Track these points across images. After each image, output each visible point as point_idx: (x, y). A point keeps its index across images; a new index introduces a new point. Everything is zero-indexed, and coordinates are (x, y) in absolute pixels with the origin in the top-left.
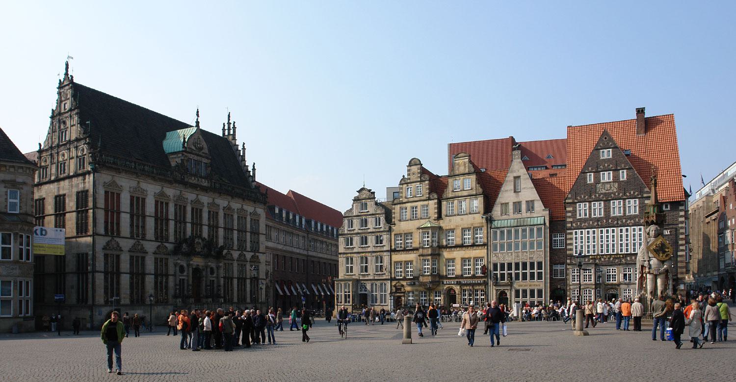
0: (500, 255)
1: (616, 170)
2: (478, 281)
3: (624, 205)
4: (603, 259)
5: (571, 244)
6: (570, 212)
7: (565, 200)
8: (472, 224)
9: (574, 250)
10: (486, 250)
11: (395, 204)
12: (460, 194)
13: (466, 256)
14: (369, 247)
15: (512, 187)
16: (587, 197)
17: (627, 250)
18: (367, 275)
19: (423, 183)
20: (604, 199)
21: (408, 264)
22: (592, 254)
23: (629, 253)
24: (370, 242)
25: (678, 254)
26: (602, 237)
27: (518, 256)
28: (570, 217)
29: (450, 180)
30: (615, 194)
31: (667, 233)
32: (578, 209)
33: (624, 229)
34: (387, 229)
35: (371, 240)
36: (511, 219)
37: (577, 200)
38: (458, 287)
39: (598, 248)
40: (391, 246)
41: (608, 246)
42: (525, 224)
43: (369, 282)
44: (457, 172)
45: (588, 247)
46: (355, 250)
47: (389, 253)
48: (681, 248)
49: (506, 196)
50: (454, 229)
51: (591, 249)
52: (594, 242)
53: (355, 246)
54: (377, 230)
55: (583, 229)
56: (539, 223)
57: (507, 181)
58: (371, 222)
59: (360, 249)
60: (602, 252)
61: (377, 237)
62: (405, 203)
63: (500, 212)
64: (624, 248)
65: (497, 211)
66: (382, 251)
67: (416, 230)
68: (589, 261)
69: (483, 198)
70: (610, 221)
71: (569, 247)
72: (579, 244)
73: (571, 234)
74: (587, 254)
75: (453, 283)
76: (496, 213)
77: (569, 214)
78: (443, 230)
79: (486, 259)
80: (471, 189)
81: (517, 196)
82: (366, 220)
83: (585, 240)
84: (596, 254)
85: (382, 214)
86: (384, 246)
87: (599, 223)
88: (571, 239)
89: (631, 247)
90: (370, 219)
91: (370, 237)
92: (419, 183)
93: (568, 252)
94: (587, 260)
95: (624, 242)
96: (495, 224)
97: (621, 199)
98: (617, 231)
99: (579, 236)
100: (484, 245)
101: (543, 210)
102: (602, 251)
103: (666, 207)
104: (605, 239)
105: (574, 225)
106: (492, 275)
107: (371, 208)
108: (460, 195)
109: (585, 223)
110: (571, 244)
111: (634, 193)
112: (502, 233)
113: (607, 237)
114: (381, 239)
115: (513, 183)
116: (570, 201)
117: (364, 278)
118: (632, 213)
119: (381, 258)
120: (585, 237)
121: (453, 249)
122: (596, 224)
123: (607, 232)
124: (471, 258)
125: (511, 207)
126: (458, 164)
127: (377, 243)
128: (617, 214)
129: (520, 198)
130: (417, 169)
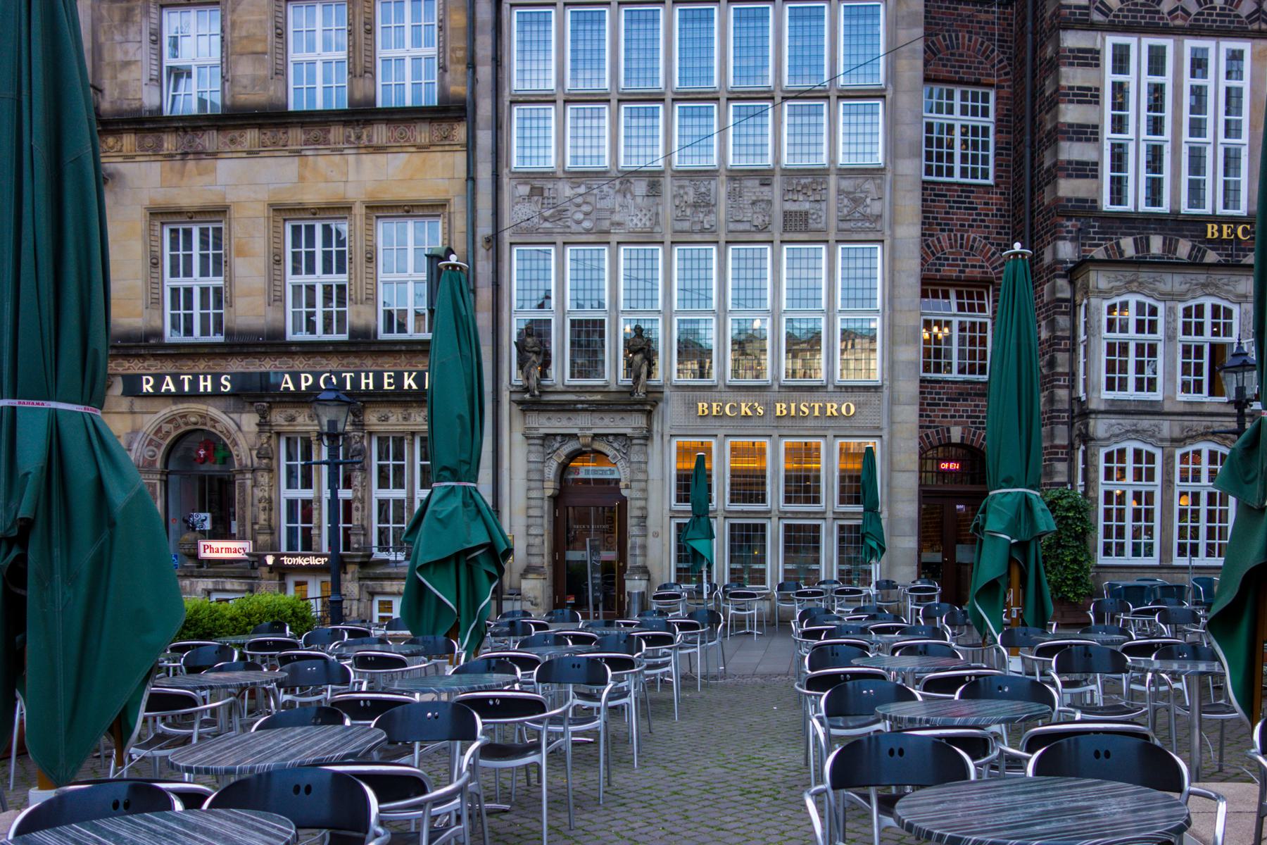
0: (566, 190)
2: (399, 378)
5: (1088, 133)
9: (1106, 173)
10: (460, 158)
13: (313, 195)
27: (704, 203)
38: (249, 421)
71: (1072, 151)
72: (1137, 136)
75: (206, 384)
79: (460, 223)
93: (1068, 188)
99: (1138, 79)
110: (1088, 133)
121: (210, 140)
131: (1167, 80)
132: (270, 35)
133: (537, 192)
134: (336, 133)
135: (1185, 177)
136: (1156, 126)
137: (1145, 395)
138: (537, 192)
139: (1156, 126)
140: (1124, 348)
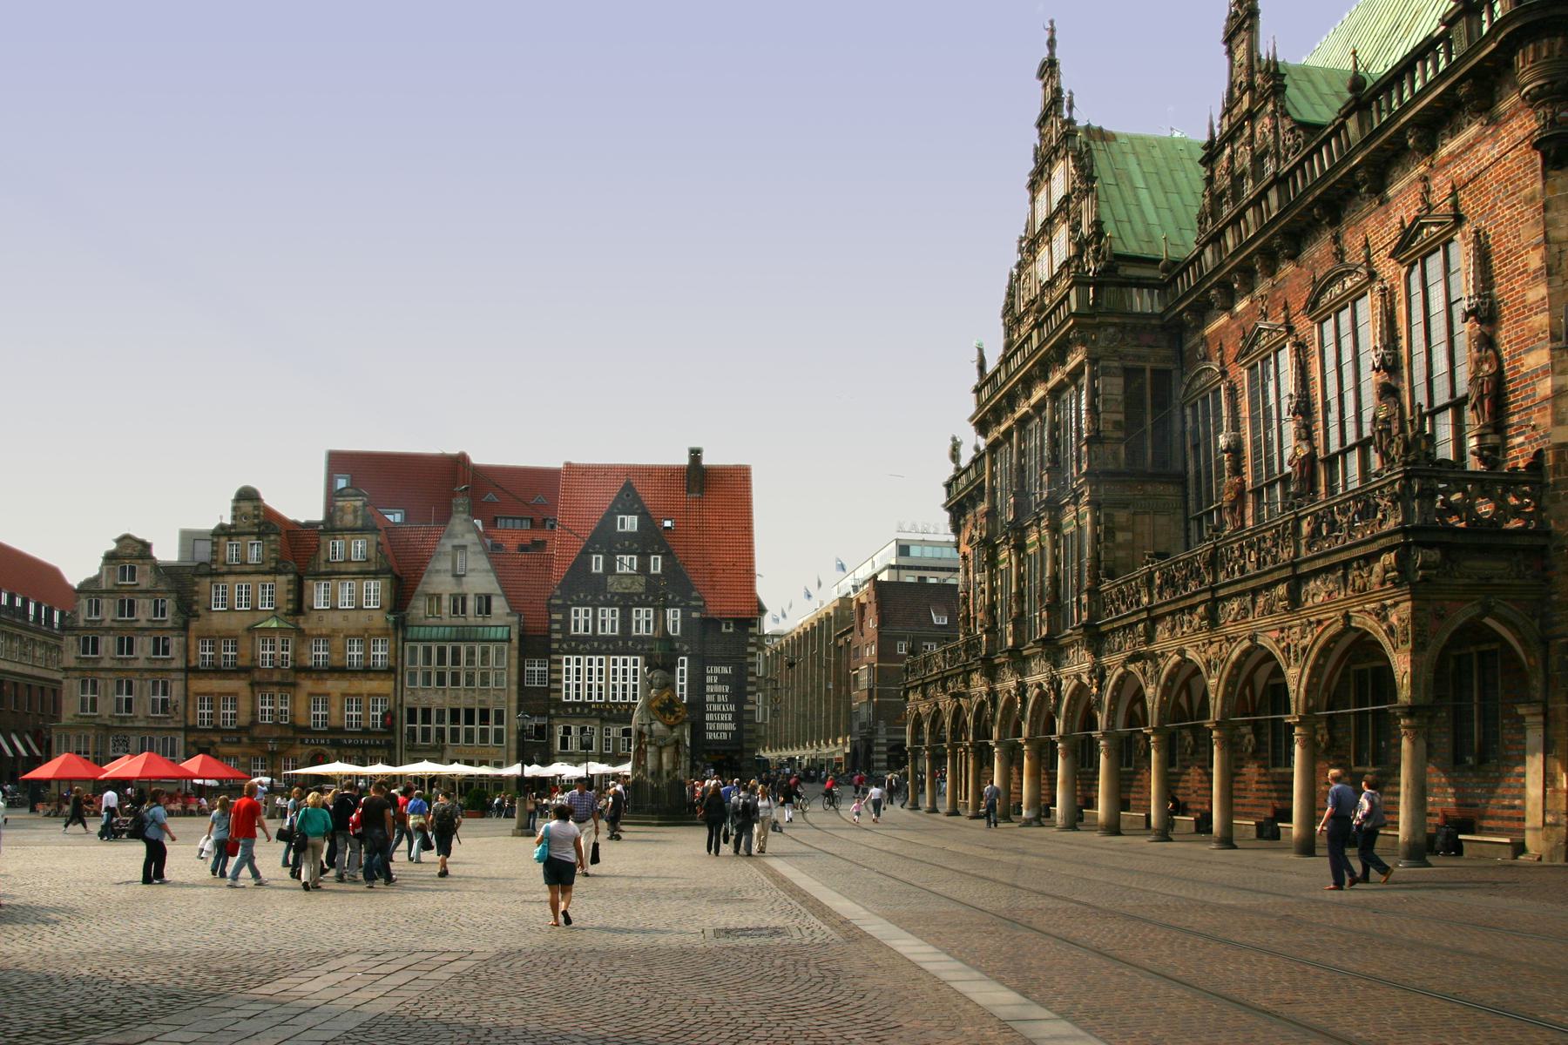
0: (421, 693)
4: (615, 711)
6: (557, 621)
8: (366, 630)
10: (392, 683)
11: (201, 576)
12: (343, 568)
13: (352, 692)
14: (137, 659)
15: (449, 566)
18: (131, 717)
19: (265, 539)
21: (225, 700)
24: (139, 648)
26: (615, 671)
27: (457, 697)
28: (557, 631)
29: (323, 539)
30: (640, 597)
34: (180, 621)
35: (144, 647)
36: (445, 626)
37: (572, 600)
39: (607, 691)
40: (188, 661)
41: (624, 687)
42: (473, 637)
43: (135, 732)
44: (338, 524)
45: (590, 687)
46: (106, 664)
47: (182, 676)
49: (439, 582)
50: (328, 636)
51: (595, 692)
53: (103, 655)
54: (157, 625)
55: (580, 654)
56: (499, 636)
57: (440, 553)
58: (143, 607)
59: (115, 662)
61: (156, 640)
62: (222, 574)
63: (423, 611)
65: (419, 608)
66: (168, 670)
67: (245, 633)
69: (389, 581)
70: (630, 643)
71: (554, 686)
73: (560, 662)
74: (586, 700)
76: (414, 611)
77: (556, 626)
78: (305, 635)
79: (392, 700)
80: (368, 560)
81: (460, 584)
82: (131, 603)
83: (584, 675)
85: (170, 591)
86: (173, 659)
87: (611, 647)
88: (560, 672)
90: (141, 601)
91: (140, 639)
92: (254, 537)
93: (553, 695)
96: (414, 632)
97: (650, 606)
100: (390, 671)
101: (508, 614)
102: (614, 696)
103: (728, 627)
104: (620, 675)
105: (565, 646)
106: (405, 731)
107: (145, 580)
108: (343, 570)
109: (585, 644)
112: (428, 651)
113: (625, 672)
114: (166, 644)
115: (450, 558)
116: (559, 602)
117: (124, 725)
119: (165, 685)
121: (325, 676)
122: (604, 647)
123: (625, 663)
124: (361, 695)
125: (446, 603)
126: (342, 509)
127: (156, 652)
129: (464, 586)
130: (251, 508)
131: (581, 667)
132: (342, 647)
133: (413, 693)
134: (359, 675)
135: (587, 692)
138: (413, 693)
139: (578, 679)
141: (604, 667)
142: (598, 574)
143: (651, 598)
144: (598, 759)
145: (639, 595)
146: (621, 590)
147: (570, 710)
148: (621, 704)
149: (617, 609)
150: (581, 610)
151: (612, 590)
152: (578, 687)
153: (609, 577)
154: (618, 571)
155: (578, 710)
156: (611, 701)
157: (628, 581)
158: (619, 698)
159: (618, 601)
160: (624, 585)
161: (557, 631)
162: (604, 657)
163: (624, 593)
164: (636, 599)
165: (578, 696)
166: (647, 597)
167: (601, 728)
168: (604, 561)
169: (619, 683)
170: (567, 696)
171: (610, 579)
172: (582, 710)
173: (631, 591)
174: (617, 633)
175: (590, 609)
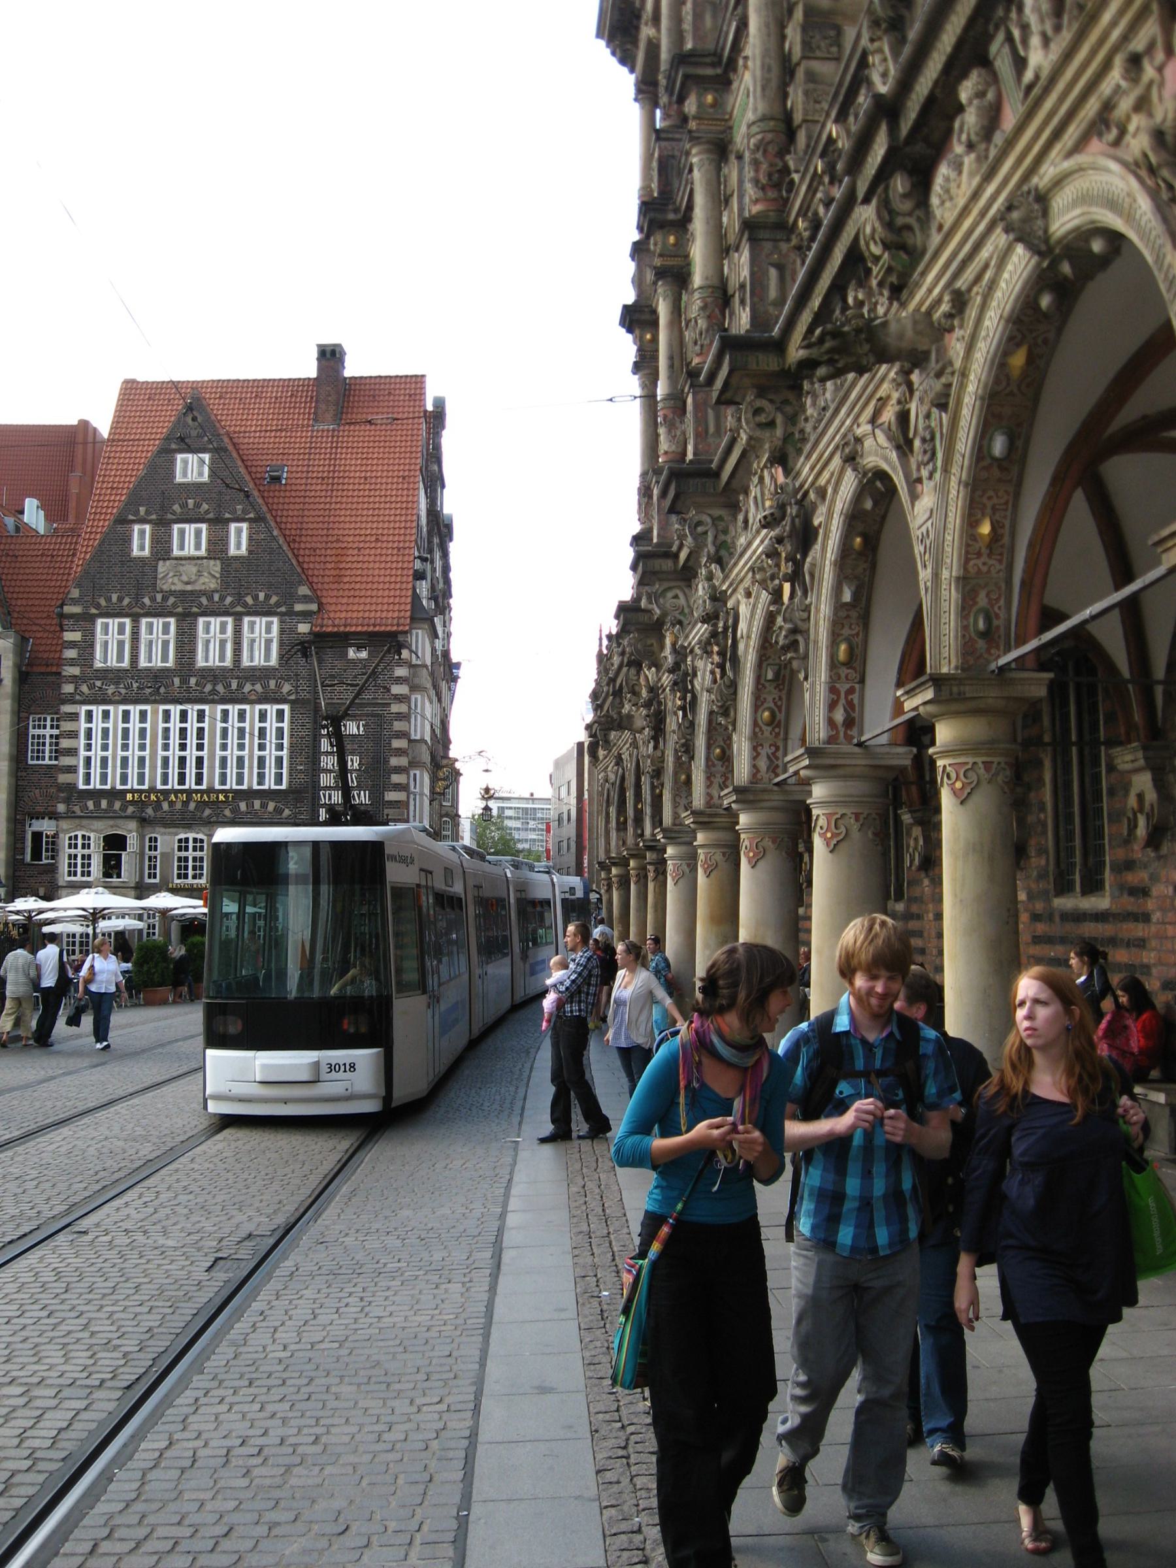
1: (219, 523)
3: (238, 632)
4: (165, 806)
6: (72, 645)
7: (61, 606)
9: (81, 771)
16: (126, 601)
17: (240, 780)
20: (180, 610)
22: (136, 787)
23: (245, 787)
25: (386, 798)
28: (72, 662)
31: (355, 731)
32: (99, 636)
33: (233, 709)
39: (153, 768)
41: (182, 760)
48: (396, 778)
51: (133, 771)
52: (142, 747)
60: (165, 782)
64: (232, 771)
68: (124, 808)
70: (193, 681)
71: (66, 761)
72: (97, 753)
73: (74, 717)
74: (119, 787)
77: (71, 654)
84: (146, 787)
88: (74, 735)
89: (251, 768)
93: (63, 778)
94: (117, 805)
95: (232, 753)
98: (212, 713)
99: (97, 725)
102: (165, 781)
105: (84, 688)
109: (117, 684)
111: (267, 597)
113: (183, 731)
116: (77, 609)
118: (259, 660)
120: (115, 729)
123: (184, 716)
128: (214, 661)
136: (105, 747)
137: (85, 879)
140: (76, 856)
141: (148, 725)
142: (141, 560)
143: (229, 600)
144: (133, 893)
145: (209, 595)
146: (179, 587)
147: (90, 804)
148: (176, 792)
149: (172, 620)
150: (113, 623)
151: (165, 587)
152: (104, 761)
153: (161, 563)
154: (176, 552)
155: (104, 804)
156: (159, 787)
157: (191, 569)
158: (173, 783)
159: (175, 605)
160: (185, 578)
161: (72, 662)
162: (148, 707)
163: (183, 593)
164: (204, 601)
165: (104, 779)
166: (222, 598)
167: (142, 838)
168: (152, 535)
169: (174, 753)
170: (87, 780)
171: (162, 567)
172: (111, 804)
173: (197, 587)
174: (170, 664)
175: (127, 621)
